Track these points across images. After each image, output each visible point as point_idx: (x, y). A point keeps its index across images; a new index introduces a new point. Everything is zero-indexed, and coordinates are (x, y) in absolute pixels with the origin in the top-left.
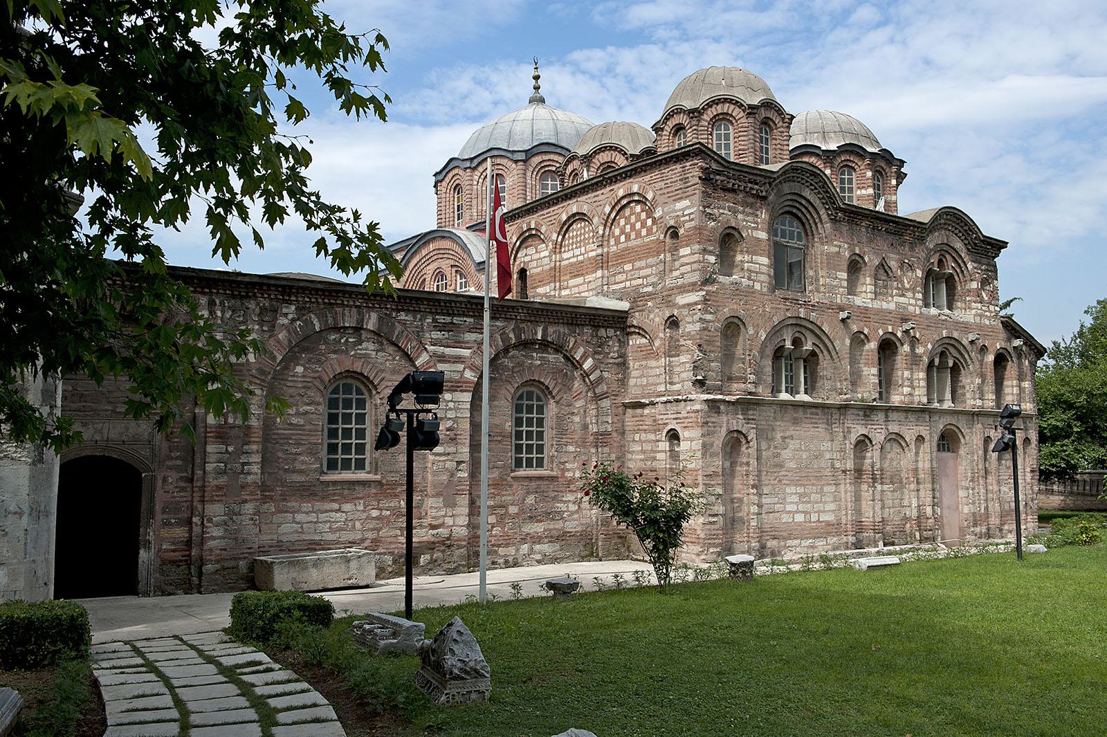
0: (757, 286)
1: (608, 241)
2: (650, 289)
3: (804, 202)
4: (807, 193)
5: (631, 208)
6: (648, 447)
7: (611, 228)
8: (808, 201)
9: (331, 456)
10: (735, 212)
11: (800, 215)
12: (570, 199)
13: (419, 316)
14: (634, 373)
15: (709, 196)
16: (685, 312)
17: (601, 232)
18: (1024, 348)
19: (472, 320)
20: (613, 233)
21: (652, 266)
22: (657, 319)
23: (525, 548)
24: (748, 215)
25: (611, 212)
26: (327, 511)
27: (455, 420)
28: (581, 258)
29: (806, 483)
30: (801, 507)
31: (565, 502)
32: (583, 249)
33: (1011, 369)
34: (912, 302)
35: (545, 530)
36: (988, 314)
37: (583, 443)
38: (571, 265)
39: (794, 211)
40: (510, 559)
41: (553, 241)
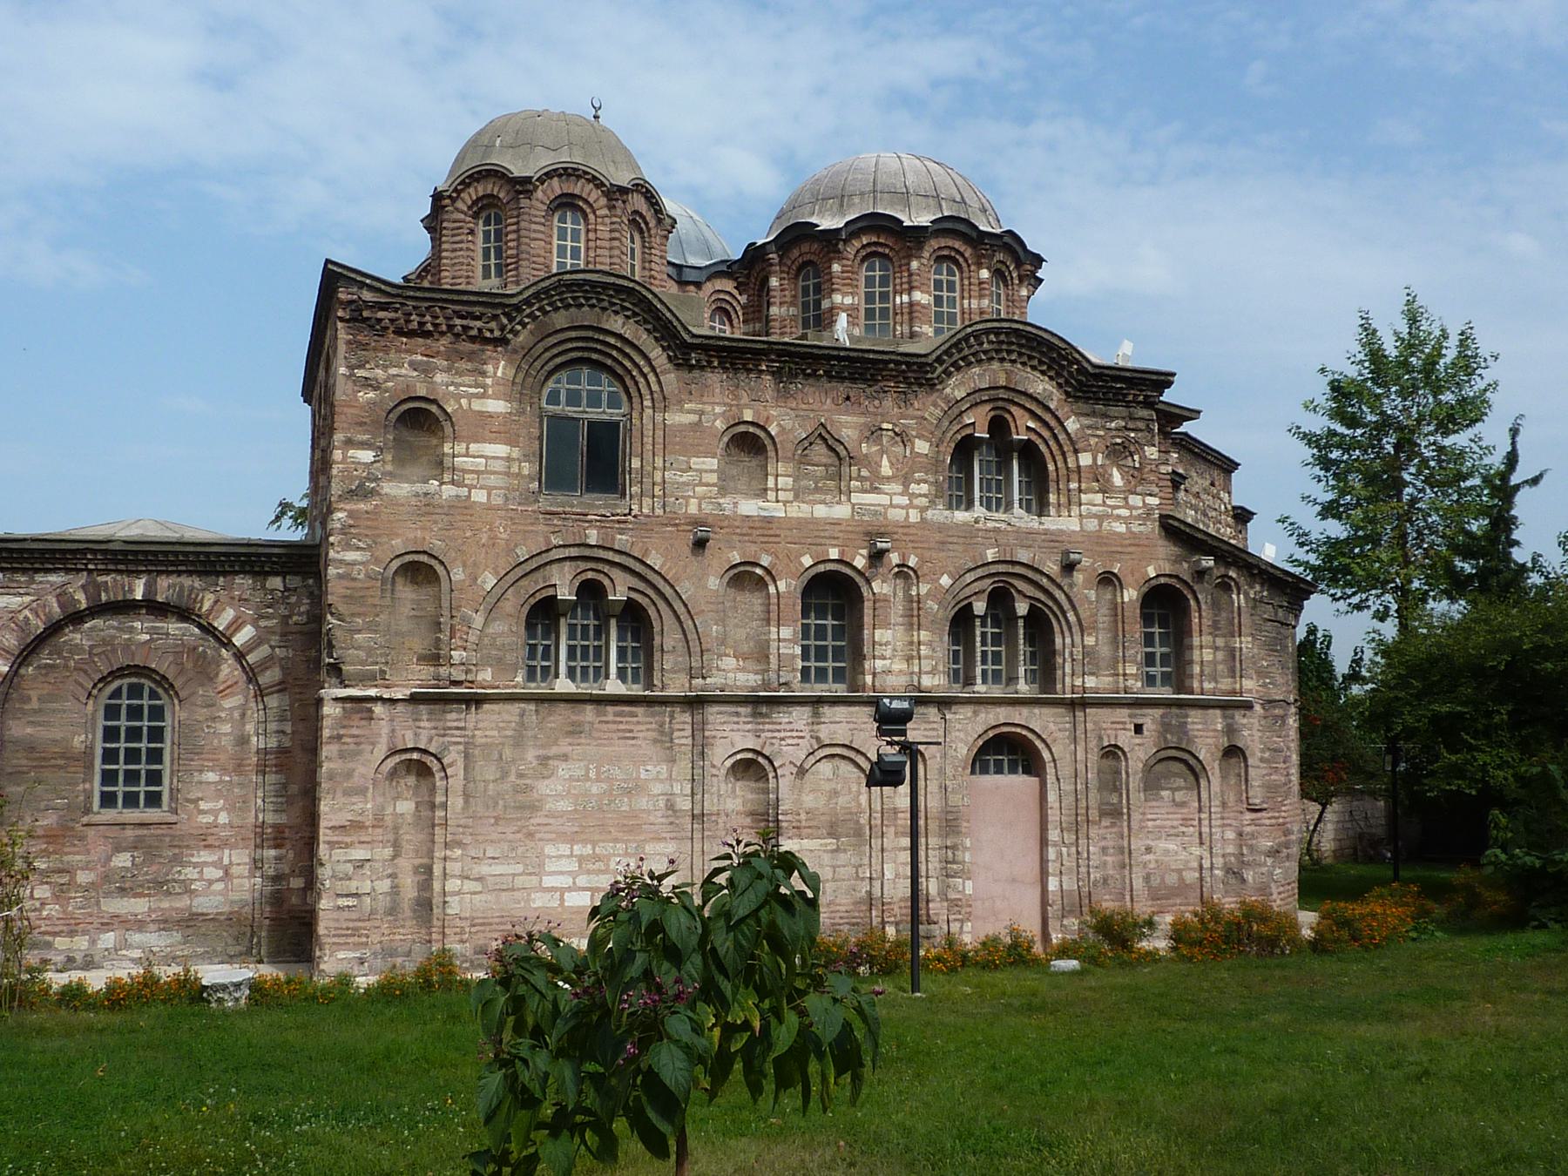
0: (479, 496)
3: (612, 341)
4: (616, 323)
8: (619, 337)
10: (426, 371)
11: (609, 362)
15: (364, 347)
23: (108, 939)
24: (459, 373)
29: (597, 837)
30: (582, 881)
31: (195, 865)
33: (1200, 617)
37: (239, 768)
40: (79, 957)
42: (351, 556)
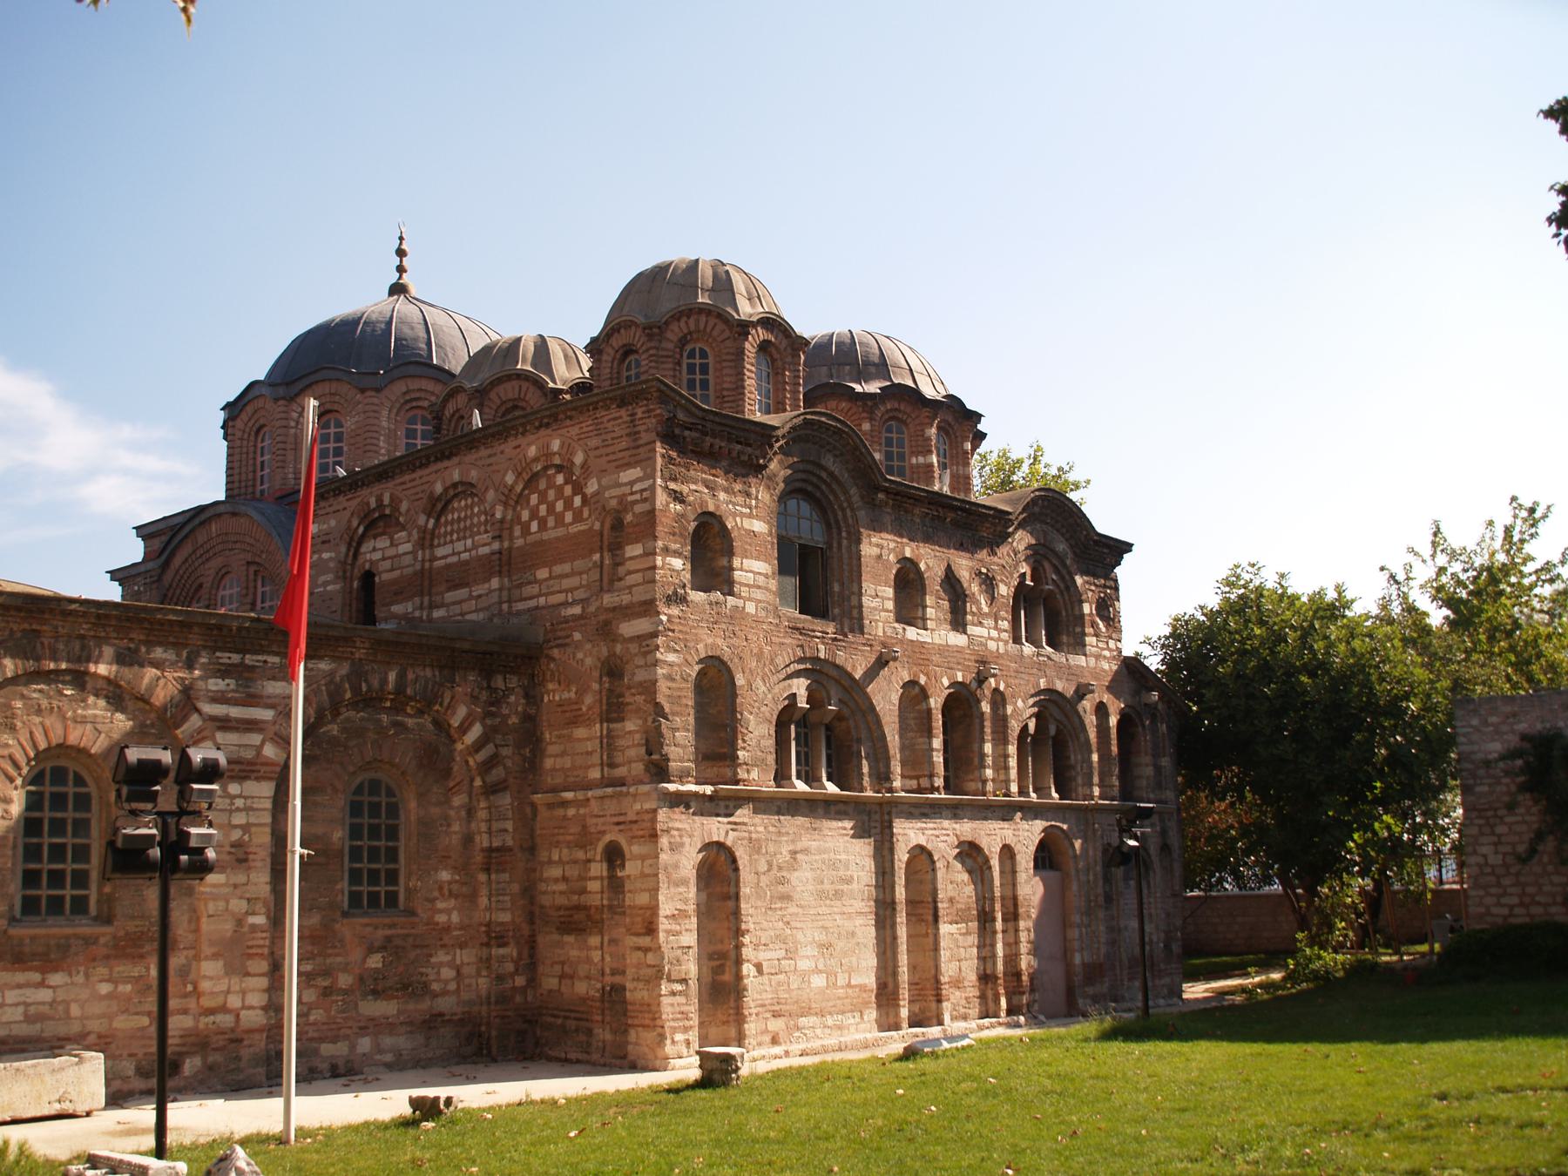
0: (751, 608)
1: (511, 529)
2: (577, 610)
3: (824, 475)
5: (549, 477)
6: (572, 872)
7: (514, 509)
8: (831, 474)
9: (29, 892)
12: (449, 458)
13: (185, 654)
14: (551, 749)
16: (633, 648)
17: (498, 515)
18: (1160, 706)
19: (276, 660)
20: (519, 518)
21: (580, 573)
22: (589, 661)
25: (516, 482)
26: (19, 986)
27: (246, 828)
28: (465, 556)
32: (469, 542)
34: (990, 632)
35: (400, 1012)
36: (1107, 653)
38: (448, 566)
39: (810, 488)
40: (341, 1063)
41: (419, 527)
42: (671, 657)
